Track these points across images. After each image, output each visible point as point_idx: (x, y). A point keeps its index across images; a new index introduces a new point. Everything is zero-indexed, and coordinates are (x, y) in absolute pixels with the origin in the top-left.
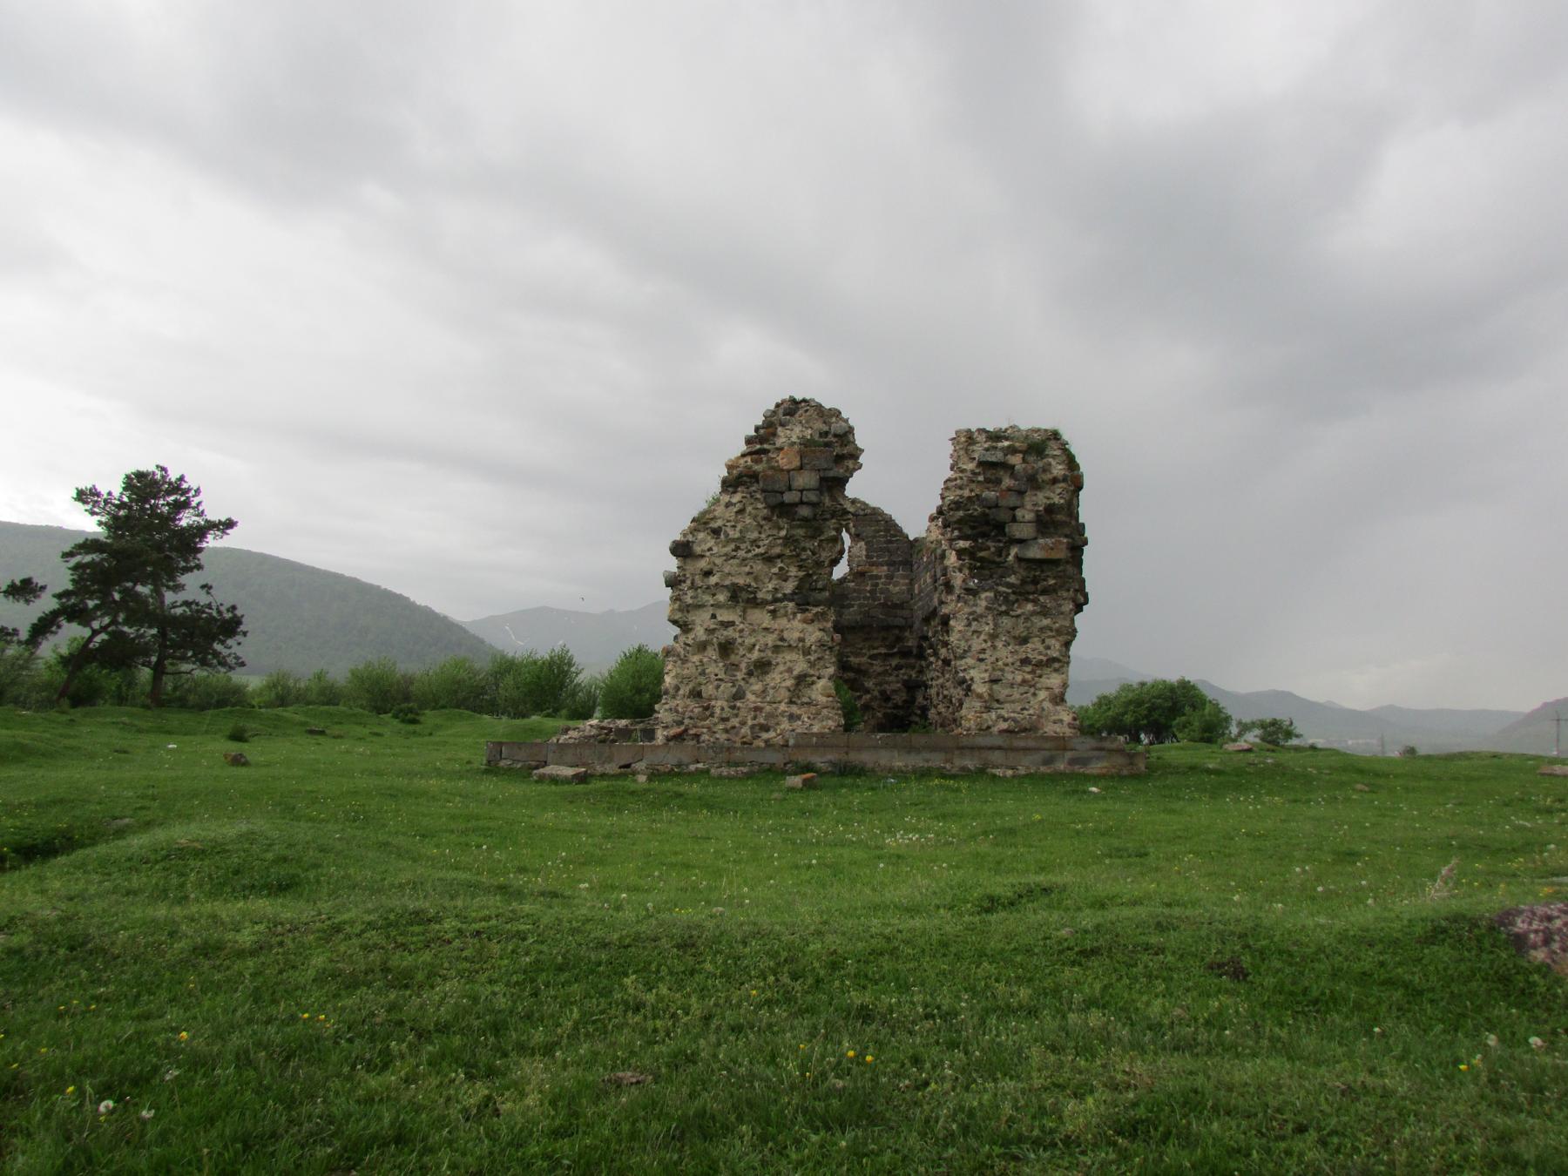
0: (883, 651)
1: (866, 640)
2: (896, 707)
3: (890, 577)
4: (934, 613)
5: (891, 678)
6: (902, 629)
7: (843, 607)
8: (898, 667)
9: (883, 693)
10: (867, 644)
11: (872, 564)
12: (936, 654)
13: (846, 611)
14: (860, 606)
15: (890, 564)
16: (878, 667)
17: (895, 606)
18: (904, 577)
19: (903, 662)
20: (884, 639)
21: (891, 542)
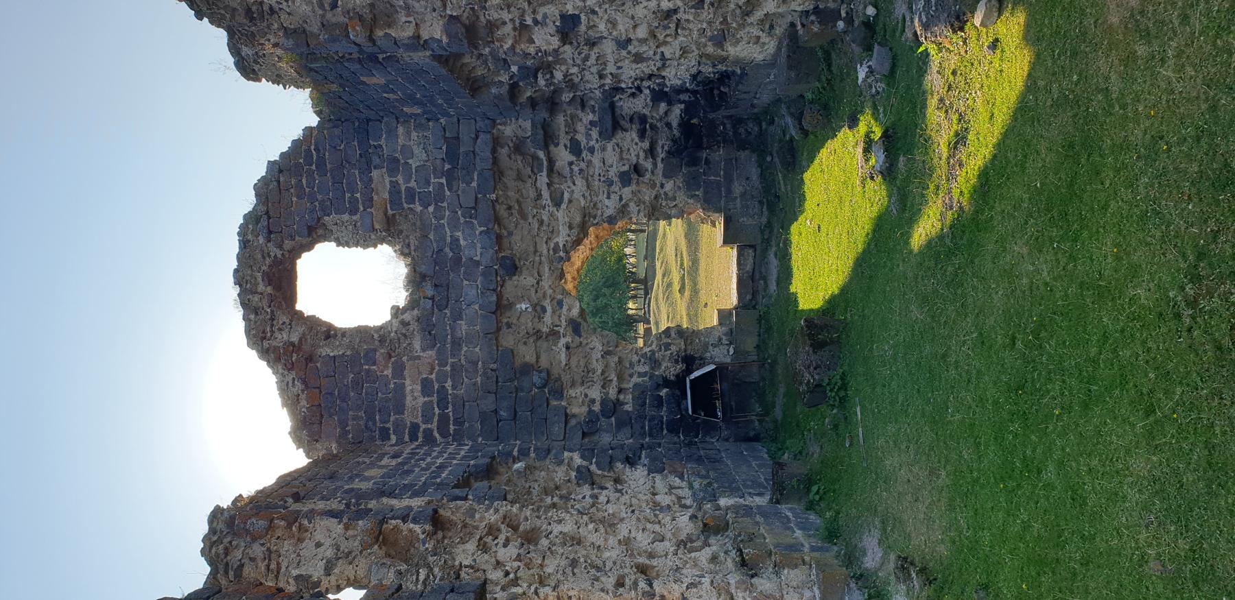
0: (543, 179)
1: (524, 216)
2: (651, 152)
3: (394, 165)
4: (447, 60)
5: (596, 161)
6: (496, 142)
7: (457, 260)
8: (575, 149)
9: (625, 179)
10: (530, 210)
11: (369, 202)
12: (545, 65)
13: (466, 254)
14: (454, 225)
15: (368, 167)
16: (576, 190)
17: (452, 156)
18: (392, 134)
19: (564, 140)
20: (519, 177)
21: (321, 163)
